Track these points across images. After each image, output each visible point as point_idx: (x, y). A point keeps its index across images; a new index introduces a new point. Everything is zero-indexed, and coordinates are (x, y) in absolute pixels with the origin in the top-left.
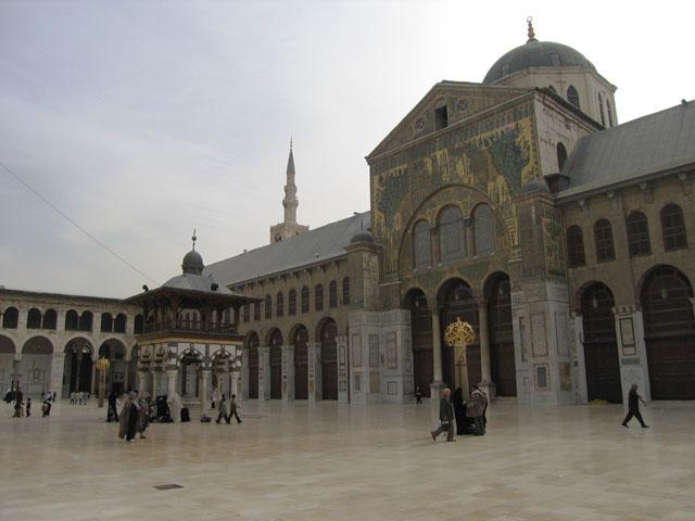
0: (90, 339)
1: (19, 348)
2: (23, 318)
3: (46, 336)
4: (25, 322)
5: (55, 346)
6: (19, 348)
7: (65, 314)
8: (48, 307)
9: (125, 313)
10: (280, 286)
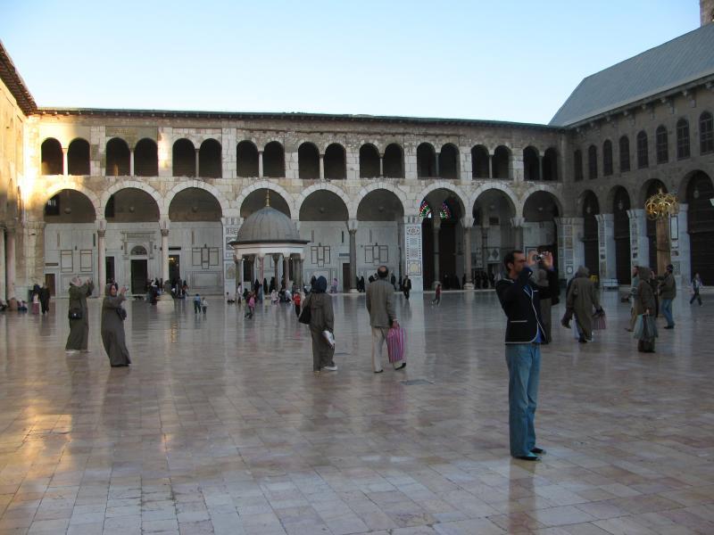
0: (457, 191)
1: (353, 210)
2: (353, 161)
3: (391, 188)
4: (357, 167)
5: (405, 204)
6: (353, 210)
7: (415, 150)
8: (389, 140)
9: (507, 145)
10: (630, 128)
